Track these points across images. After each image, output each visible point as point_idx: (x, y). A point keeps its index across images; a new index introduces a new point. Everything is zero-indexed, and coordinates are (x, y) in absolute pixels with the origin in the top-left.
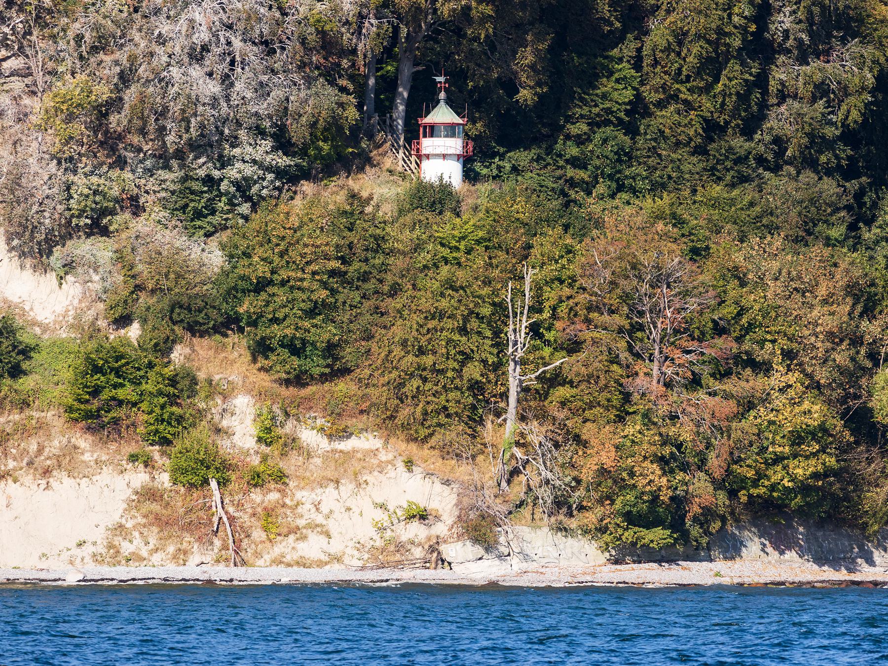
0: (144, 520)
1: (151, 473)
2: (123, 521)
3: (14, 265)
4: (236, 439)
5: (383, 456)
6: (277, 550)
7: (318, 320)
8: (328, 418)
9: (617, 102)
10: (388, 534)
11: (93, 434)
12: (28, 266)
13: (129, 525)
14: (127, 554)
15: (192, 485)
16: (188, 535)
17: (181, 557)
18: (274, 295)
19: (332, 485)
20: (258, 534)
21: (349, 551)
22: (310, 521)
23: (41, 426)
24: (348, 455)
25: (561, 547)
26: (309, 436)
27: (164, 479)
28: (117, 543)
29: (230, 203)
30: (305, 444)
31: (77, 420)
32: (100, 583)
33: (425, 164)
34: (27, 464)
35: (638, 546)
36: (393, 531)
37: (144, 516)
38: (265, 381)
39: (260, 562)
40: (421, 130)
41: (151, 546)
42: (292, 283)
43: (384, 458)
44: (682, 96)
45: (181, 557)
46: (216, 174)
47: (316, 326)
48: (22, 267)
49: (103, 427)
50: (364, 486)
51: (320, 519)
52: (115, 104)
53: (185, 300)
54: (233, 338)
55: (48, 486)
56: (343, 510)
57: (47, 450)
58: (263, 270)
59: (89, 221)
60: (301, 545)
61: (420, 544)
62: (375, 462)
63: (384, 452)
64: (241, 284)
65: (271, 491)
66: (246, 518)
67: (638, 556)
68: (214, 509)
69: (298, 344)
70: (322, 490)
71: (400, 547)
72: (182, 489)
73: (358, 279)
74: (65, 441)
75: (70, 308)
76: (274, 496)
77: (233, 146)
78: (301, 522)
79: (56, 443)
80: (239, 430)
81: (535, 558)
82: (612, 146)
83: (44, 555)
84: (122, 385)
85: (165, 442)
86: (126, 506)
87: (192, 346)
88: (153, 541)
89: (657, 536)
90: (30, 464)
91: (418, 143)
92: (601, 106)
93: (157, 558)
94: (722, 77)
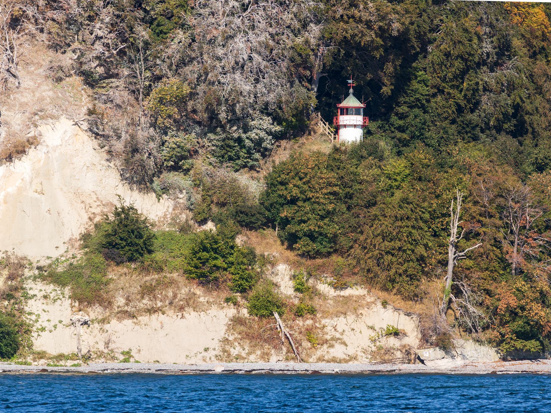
0: (239, 336)
1: (237, 309)
2: (226, 336)
3: (126, 188)
4: (282, 289)
5: (369, 299)
6: (319, 353)
7: (326, 220)
8: (335, 277)
9: (422, 95)
10: (378, 344)
11: (203, 286)
12: (135, 188)
13: (231, 338)
14: (234, 355)
15: (262, 316)
16: (267, 345)
17: (265, 356)
18: (302, 206)
19: (343, 316)
20: (306, 344)
21: (359, 353)
22: (332, 336)
23: (172, 282)
24: (347, 299)
25: (479, 351)
26: (323, 288)
27: (245, 312)
28: (228, 349)
29: (249, 152)
30: (321, 292)
31: (194, 278)
32: (285, 372)
33: (342, 131)
34: (169, 304)
35: (524, 351)
36: (380, 342)
37: (240, 333)
38: (290, 255)
39: (311, 360)
40: (339, 111)
41: (247, 351)
42: (313, 200)
43: (369, 300)
44: (446, 90)
45: (265, 356)
46: (244, 136)
47: (325, 224)
48: (132, 189)
49: (209, 282)
50: (360, 316)
51: (338, 335)
52: (192, 95)
53: (243, 209)
54: (268, 232)
55: (183, 317)
56: (350, 330)
57: (179, 296)
58: (295, 192)
59: (173, 164)
60: (331, 350)
61: (398, 350)
62: (364, 302)
63: (368, 297)
64: (281, 200)
65: (307, 319)
66: (296, 334)
67: (513, 356)
68: (279, 329)
69: (316, 235)
70: (337, 319)
71: (388, 351)
72: (256, 318)
73: (346, 197)
74: (187, 290)
75: (167, 213)
76: (309, 322)
77: (253, 120)
78: (328, 337)
79: (183, 291)
80: (283, 284)
81: (468, 357)
82: (421, 120)
83: (187, 356)
84: (216, 258)
85: (243, 291)
86: (227, 328)
87: (246, 235)
88: (247, 348)
89: (532, 345)
90: (171, 303)
91: (337, 119)
92: (414, 97)
93: (252, 357)
94: (466, 79)
